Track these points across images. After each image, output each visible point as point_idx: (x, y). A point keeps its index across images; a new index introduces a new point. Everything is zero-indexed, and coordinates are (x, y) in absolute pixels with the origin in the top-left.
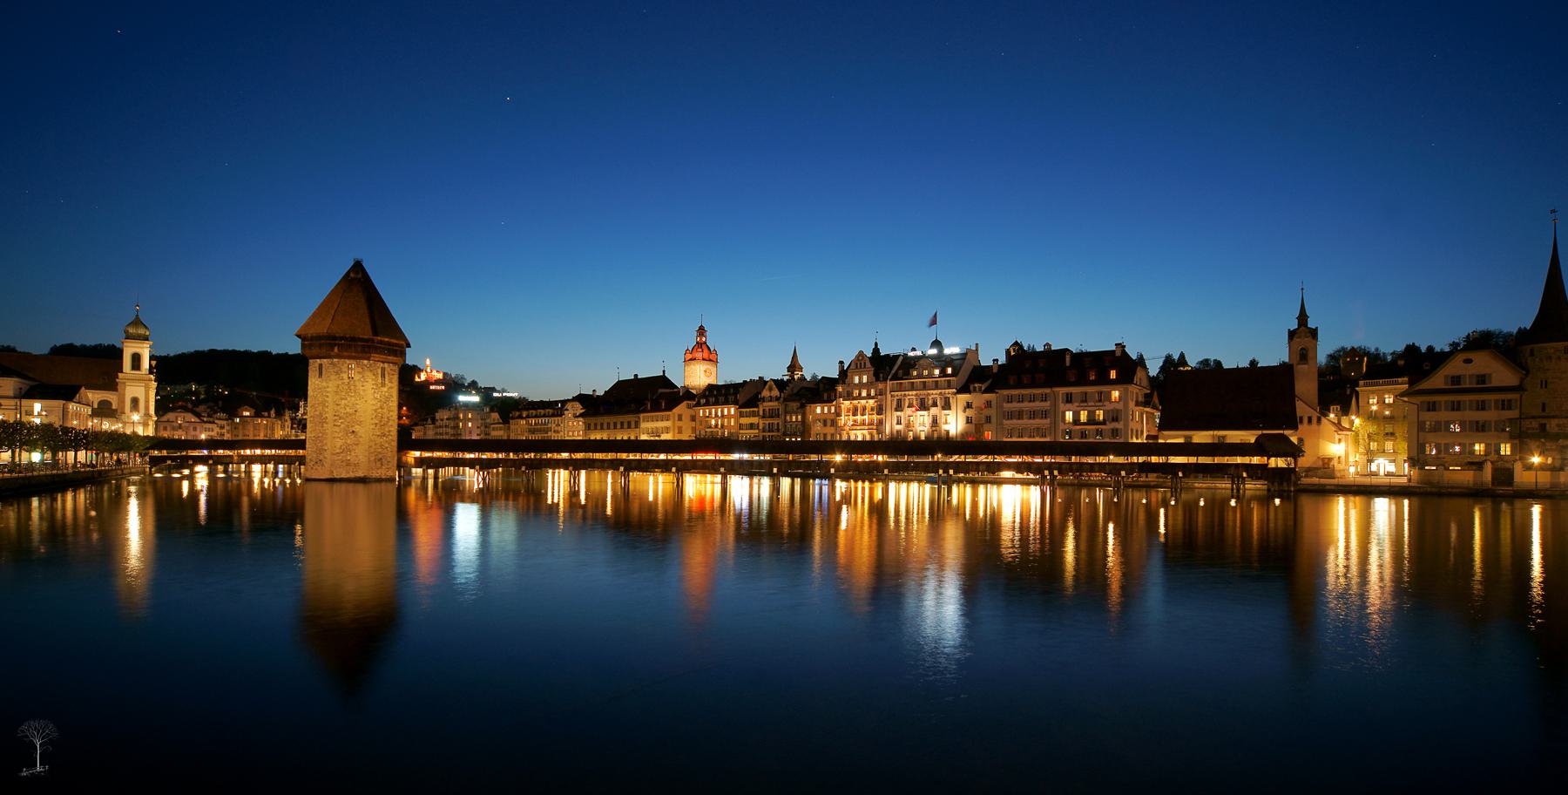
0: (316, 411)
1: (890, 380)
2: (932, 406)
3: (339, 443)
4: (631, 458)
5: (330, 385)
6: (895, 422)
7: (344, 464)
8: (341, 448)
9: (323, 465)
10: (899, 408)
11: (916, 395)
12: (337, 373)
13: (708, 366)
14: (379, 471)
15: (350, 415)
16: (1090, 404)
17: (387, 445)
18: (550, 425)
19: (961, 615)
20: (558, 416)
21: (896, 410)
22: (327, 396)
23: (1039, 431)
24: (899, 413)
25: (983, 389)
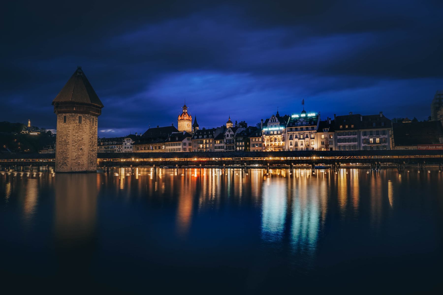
0: (62, 139)
1: (287, 127)
2: (306, 138)
3: (75, 154)
4: (256, 159)
5: (70, 126)
6: (290, 144)
7: (77, 164)
8: (75, 157)
9: (67, 165)
10: (291, 138)
11: (299, 133)
12: (74, 120)
13: (189, 122)
14: (91, 168)
15: (80, 140)
16: (374, 136)
17: (94, 155)
18: (115, 149)
19: (292, 218)
20: (119, 144)
21: (290, 139)
22: (69, 132)
23: (354, 146)
24: (291, 141)
25: (328, 130)
